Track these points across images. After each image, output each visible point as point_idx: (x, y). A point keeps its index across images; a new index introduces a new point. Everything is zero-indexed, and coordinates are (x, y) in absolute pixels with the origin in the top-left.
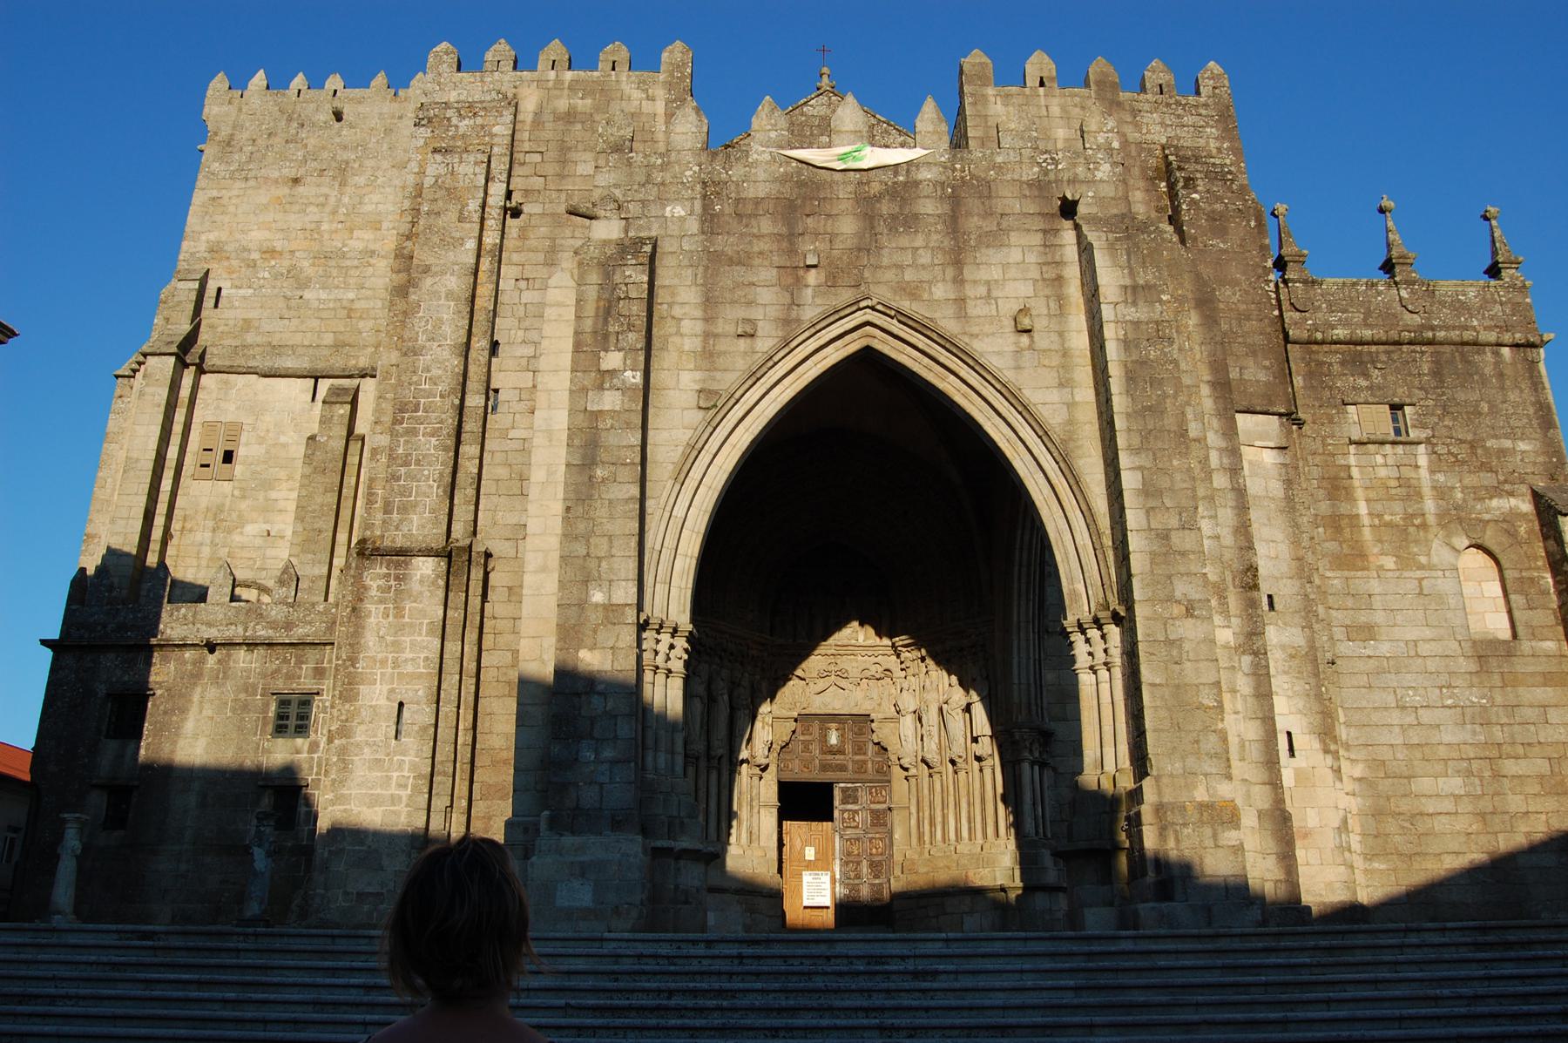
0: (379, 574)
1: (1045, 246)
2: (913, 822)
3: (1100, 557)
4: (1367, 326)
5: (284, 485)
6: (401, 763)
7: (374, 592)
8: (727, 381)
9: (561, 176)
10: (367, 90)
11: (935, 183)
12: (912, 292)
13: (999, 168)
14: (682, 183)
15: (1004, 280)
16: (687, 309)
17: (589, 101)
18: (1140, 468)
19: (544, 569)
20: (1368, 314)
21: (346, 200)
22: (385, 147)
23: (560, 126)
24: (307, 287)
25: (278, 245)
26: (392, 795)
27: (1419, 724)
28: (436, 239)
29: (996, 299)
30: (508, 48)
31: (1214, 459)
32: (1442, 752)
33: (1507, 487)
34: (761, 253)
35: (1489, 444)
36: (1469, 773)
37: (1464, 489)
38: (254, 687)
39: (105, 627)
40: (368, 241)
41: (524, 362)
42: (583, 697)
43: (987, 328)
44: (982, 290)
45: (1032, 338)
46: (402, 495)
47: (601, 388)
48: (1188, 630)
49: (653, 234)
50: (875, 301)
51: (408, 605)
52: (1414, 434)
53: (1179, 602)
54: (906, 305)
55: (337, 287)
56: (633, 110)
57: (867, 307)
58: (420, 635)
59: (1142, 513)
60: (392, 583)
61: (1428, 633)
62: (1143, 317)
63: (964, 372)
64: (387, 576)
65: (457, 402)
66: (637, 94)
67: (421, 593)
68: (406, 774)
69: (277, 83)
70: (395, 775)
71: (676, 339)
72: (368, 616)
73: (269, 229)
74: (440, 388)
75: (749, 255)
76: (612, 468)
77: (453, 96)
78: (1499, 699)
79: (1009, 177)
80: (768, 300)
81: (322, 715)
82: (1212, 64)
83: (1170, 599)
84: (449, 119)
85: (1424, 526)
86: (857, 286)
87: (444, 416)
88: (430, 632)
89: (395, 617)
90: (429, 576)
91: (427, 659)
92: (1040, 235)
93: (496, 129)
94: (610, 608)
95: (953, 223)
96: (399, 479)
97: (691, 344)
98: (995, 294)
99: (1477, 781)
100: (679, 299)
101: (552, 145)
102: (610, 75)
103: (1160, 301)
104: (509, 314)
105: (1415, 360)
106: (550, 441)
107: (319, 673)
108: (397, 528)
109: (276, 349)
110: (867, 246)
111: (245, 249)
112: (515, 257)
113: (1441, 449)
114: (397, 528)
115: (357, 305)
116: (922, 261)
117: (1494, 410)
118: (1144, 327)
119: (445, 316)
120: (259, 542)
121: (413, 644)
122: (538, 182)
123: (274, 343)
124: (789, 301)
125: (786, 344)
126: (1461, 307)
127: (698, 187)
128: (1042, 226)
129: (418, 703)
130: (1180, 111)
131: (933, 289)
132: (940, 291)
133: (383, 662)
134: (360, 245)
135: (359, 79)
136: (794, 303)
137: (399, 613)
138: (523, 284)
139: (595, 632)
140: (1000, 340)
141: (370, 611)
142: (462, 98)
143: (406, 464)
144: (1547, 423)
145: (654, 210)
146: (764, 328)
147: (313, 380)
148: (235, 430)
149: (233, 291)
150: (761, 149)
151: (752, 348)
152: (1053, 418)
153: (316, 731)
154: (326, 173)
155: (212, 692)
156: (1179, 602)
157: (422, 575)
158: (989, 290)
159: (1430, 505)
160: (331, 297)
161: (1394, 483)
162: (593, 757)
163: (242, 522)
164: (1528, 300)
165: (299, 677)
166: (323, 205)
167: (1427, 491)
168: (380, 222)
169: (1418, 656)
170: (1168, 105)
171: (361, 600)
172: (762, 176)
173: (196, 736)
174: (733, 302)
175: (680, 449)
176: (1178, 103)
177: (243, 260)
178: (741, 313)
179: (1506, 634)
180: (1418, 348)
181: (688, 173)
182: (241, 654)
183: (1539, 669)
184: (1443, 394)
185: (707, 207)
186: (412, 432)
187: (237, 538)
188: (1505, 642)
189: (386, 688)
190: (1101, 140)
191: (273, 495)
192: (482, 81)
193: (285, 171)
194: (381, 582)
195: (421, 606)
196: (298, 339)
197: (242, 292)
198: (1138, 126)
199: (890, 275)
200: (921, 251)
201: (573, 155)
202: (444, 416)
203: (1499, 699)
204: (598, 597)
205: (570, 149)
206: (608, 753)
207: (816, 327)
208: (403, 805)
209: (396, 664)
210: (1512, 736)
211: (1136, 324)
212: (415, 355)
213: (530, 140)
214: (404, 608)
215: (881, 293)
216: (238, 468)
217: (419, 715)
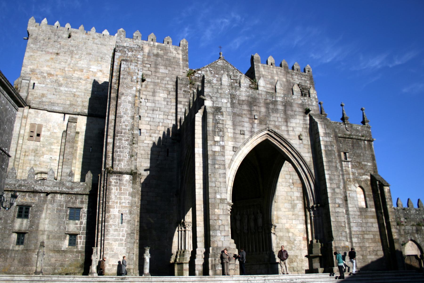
5: (56, 145)
6: (123, 230)
7: (113, 183)
8: (239, 145)
9: (156, 72)
10: (78, 30)
11: (281, 102)
12: (278, 127)
13: (294, 99)
16: (229, 126)
17: (162, 52)
18: (328, 174)
21: (73, 62)
22: (84, 48)
23: (155, 58)
24: (61, 86)
25: (52, 72)
26: (121, 239)
28: (125, 86)
29: (295, 131)
30: (140, 33)
33: (366, 173)
34: (245, 114)
36: (358, 238)
37: (358, 173)
38: (63, 205)
39: (15, 185)
40: (80, 75)
41: (147, 122)
42: (217, 221)
44: (291, 129)
45: (302, 141)
46: (119, 157)
47: (215, 145)
48: (338, 210)
51: (123, 187)
52: (348, 159)
53: (337, 204)
54: (276, 130)
55: (70, 87)
56: (174, 56)
58: (126, 196)
59: (329, 184)
60: (118, 181)
62: (328, 140)
63: (288, 148)
66: (175, 52)
68: (124, 233)
69: (51, 23)
70: (121, 233)
72: (112, 189)
73: (49, 67)
74: (128, 128)
75: (242, 114)
76: (219, 165)
77: (125, 45)
79: (296, 102)
80: (247, 126)
81: (83, 214)
82: (308, 65)
83: (335, 203)
84: (125, 51)
85: (350, 181)
86: (266, 125)
87: (129, 136)
89: (119, 190)
91: (128, 202)
93: (139, 56)
94: (221, 199)
95: (285, 111)
96: (118, 152)
97: (231, 135)
98: (295, 130)
99: (359, 239)
101: (153, 63)
102: (167, 45)
104: (143, 108)
109: (53, 104)
110: (268, 115)
111: (42, 72)
112: (144, 93)
113: (353, 164)
114: (118, 166)
115: (77, 93)
117: (363, 154)
118: (328, 143)
119: (128, 108)
120: (49, 160)
121: (125, 198)
122: (149, 73)
123: (52, 102)
124: (251, 127)
125: (251, 136)
126: (357, 131)
127: (229, 95)
129: (126, 214)
130: (301, 76)
132: (283, 128)
133: (117, 203)
134: (77, 76)
135: (75, 26)
136: (253, 127)
137: (120, 189)
138: (146, 101)
139: (218, 205)
142: (128, 45)
143: (119, 148)
144: (373, 158)
145: (219, 100)
146: (247, 133)
147: (63, 115)
148: (40, 127)
149: (39, 84)
151: (244, 137)
153: (82, 219)
154: (66, 53)
155: (50, 206)
157: (126, 180)
158: (293, 129)
159: (351, 176)
160: (69, 90)
163: (43, 154)
164: (370, 130)
165: (76, 203)
166: (66, 62)
167: (351, 173)
168: (83, 70)
170: (299, 74)
172: (244, 95)
173: (45, 219)
174: (239, 126)
176: (301, 74)
177: (42, 76)
178: (241, 128)
179: (365, 207)
180: (349, 139)
181: (227, 91)
182: (59, 195)
183: (371, 215)
184: (354, 151)
185: (232, 101)
187: (42, 159)
188: (365, 208)
189: (118, 210)
190: (313, 96)
191: (53, 147)
192: (133, 41)
193: (54, 50)
194: (115, 181)
195: (126, 188)
196: (59, 101)
197: (41, 85)
198: (293, 78)
199: (273, 123)
200: (279, 118)
201: (158, 66)
202: (129, 136)
203: (364, 221)
204: (218, 196)
205: (158, 65)
206: (223, 234)
207: (257, 133)
209: (120, 203)
210: (366, 229)
211: (327, 141)
212: (120, 118)
213: (147, 60)
214: (122, 188)
215: (271, 127)
216: (42, 139)
217: (127, 217)
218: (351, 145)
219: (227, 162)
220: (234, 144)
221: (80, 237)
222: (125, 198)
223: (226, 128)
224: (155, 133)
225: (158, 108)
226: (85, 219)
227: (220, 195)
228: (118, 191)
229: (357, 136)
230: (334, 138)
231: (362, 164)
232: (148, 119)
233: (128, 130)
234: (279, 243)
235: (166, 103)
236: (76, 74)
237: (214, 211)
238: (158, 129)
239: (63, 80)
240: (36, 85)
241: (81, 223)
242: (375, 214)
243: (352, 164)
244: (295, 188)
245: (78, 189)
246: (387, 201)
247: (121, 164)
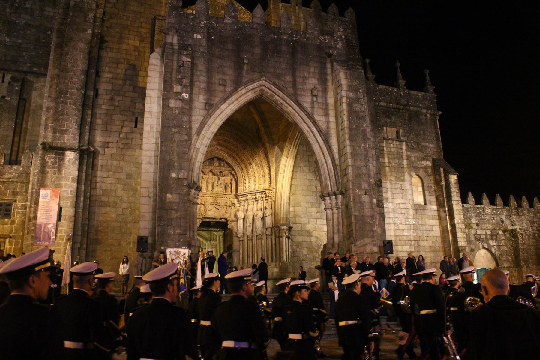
0: (52, 157)
2: (241, 256)
3: (336, 173)
4: (391, 103)
7: (50, 164)
13: (308, 39)
14: (200, 26)
19: (150, 163)
20: (391, 98)
27: (399, 229)
32: (405, 238)
33: (426, 158)
35: (422, 144)
36: (411, 245)
41: (108, 80)
43: (303, 93)
44: (302, 79)
49: (190, 43)
52: (402, 138)
58: (69, 181)
60: (57, 161)
61: (402, 201)
64: (55, 158)
65: (83, 92)
67: (69, 165)
68: (63, 234)
71: (197, 83)
72: (48, 173)
78: (420, 223)
85: (403, 168)
88: (73, 181)
89: (58, 174)
90: (72, 159)
91: (71, 191)
94: (178, 179)
95: (293, 54)
96: (59, 120)
97: (203, 85)
100: (199, 69)
103: (359, 92)
105: (403, 115)
106: (151, 116)
107: (15, 194)
108: (58, 140)
113: (409, 144)
117: (424, 133)
125: (236, 90)
127: (206, 29)
129: (68, 208)
131: (286, 77)
141: (48, 171)
143: (62, 115)
146: (229, 83)
150: (229, 18)
152: (323, 126)
157: (69, 159)
159: (405, 162)
161: (395, 153)
162: (173, 232)
167: (405, 157)
169: (399, 208)
171: (44, 167)
179: (423, 203)
180: (404, 111)
181: (202, 23)
184: (411, 127)
186: (65, 103)
195: (69, 171)
204: (174, 175)
206: (178, 231)
208: (62, 246)
214: (62, 171)
218: (407, 118)
219: (196, 126)
221: (10, 242)
222: (66, 185)
223: (197, 75)
224: (119, 95)
225: (126, 61)
226: (18, 217)
228: (57, 175)
229: (415, 106)
230: (365, 95)
231: (422, 146)
232: (111, 76)
233: (77, 89)
234: (297, 251)
235: (137, 54)
236: (23, 18)
237: (166, 196)
238: (124, 90)
241: (13, 222)
242: (436, 213)
243: (407, 145)
245: (9, 176)
246: (452, 195)
247: (65, 137)
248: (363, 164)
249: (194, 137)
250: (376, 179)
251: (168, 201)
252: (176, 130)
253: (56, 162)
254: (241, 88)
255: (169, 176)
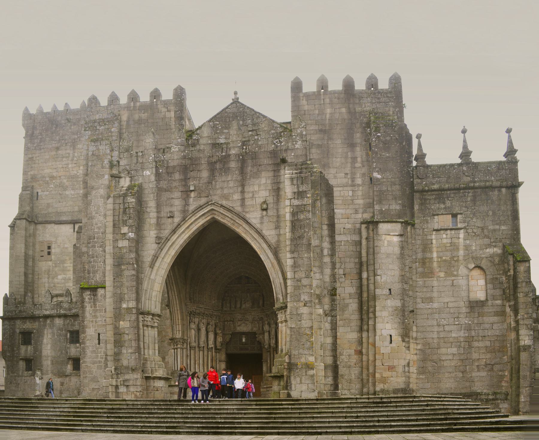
1: (274, 176)
12: (226, 197)
15: (259, 190)
31: (326, 252)
43: (252, 209)
44: (251, 195)
50: (214, 202)
53: (302, 302)
54: (224, 203)
57: (212, 204)
83: (299, 301)
86: (207, 197)
92: (272, 172)
94: (128, 309)
95: (242, 170)
97: (153, 221)
116: (231, 185)
128: (274, 169)
131: (234, 196)
136: (187, 204)
140: (256, 213)
151: (173, 221)
152: (273, 240)
156: (302, 302)
158: (253, 195)
174: (166, 205)
175: (151, 257)
199: (219, 192)
204: (124, 306)
207: (194, 212)
215: (215, 199)
220: (158, 234)
227: (127, 303)
239: (67, 181)
240: (39, 194)
244: (348, 282)
248: (304, 276)
249: (147, 270)
250: (329, 288)
251: (121, 327)
252: (125, 267)
253: (92, 298)
254: (189, 217)
255: (121, 307)
